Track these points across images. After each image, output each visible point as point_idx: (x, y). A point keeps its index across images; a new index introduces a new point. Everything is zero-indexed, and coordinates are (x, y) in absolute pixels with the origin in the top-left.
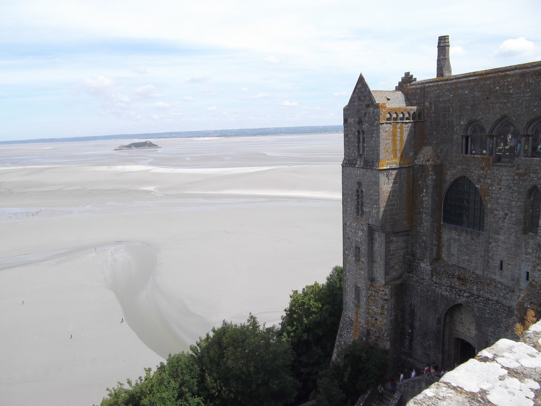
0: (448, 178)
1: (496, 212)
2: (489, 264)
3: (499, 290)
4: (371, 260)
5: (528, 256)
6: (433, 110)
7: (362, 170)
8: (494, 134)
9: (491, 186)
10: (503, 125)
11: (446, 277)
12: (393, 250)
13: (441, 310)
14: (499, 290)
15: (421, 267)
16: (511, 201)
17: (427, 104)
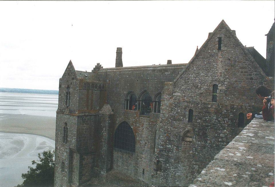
0: (117, 122)
4: (71, 171)
7: (68, 116)
8: (140, 99)
12: (85, 164)
17: (108, 81)
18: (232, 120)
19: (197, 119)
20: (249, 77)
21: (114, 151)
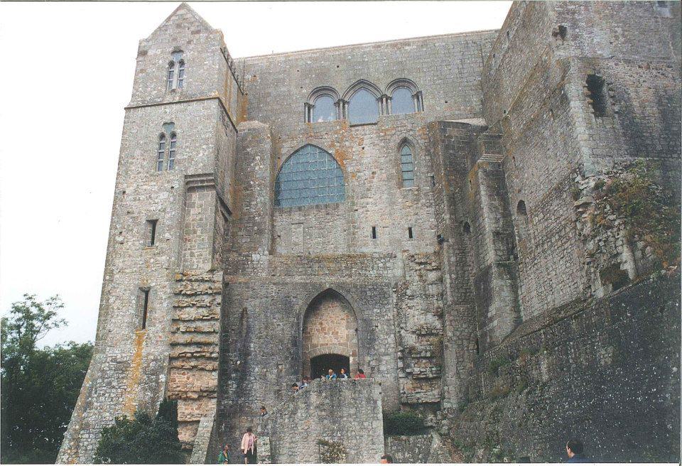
0: (284, 151)
15: (252, 261)
21: (277, 214)
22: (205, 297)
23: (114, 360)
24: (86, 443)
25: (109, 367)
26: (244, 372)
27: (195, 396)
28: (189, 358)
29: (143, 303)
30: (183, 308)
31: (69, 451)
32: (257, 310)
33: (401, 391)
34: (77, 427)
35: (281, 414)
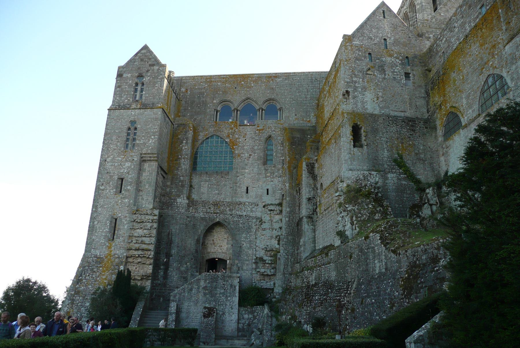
1: (242, 155)
2: (237, 192)
3: (247, 206)
5: (267, 178)
6: (189, 94)
9: (238, 139)
10: (245, 105)
11: (203, 206)
13: (200, 231)
14: (247, 206)
15: (177, 203)
16: (254, 146)
18: (401, 60)
19: (376, 60)
20: (408, 36)
21: (193, 175)
22: (148, 223)
23: (96, 256)
24: (77, 302)
25: (92, 260)
26: (167, 265)
27: (140, 278)
28: (137, 257)
29: (113, 225)
30: (135, 229)
31: (68, 306)
32: (177, 231)
33: (253, 281)
34: (73, 293)
35: (184, 291)
